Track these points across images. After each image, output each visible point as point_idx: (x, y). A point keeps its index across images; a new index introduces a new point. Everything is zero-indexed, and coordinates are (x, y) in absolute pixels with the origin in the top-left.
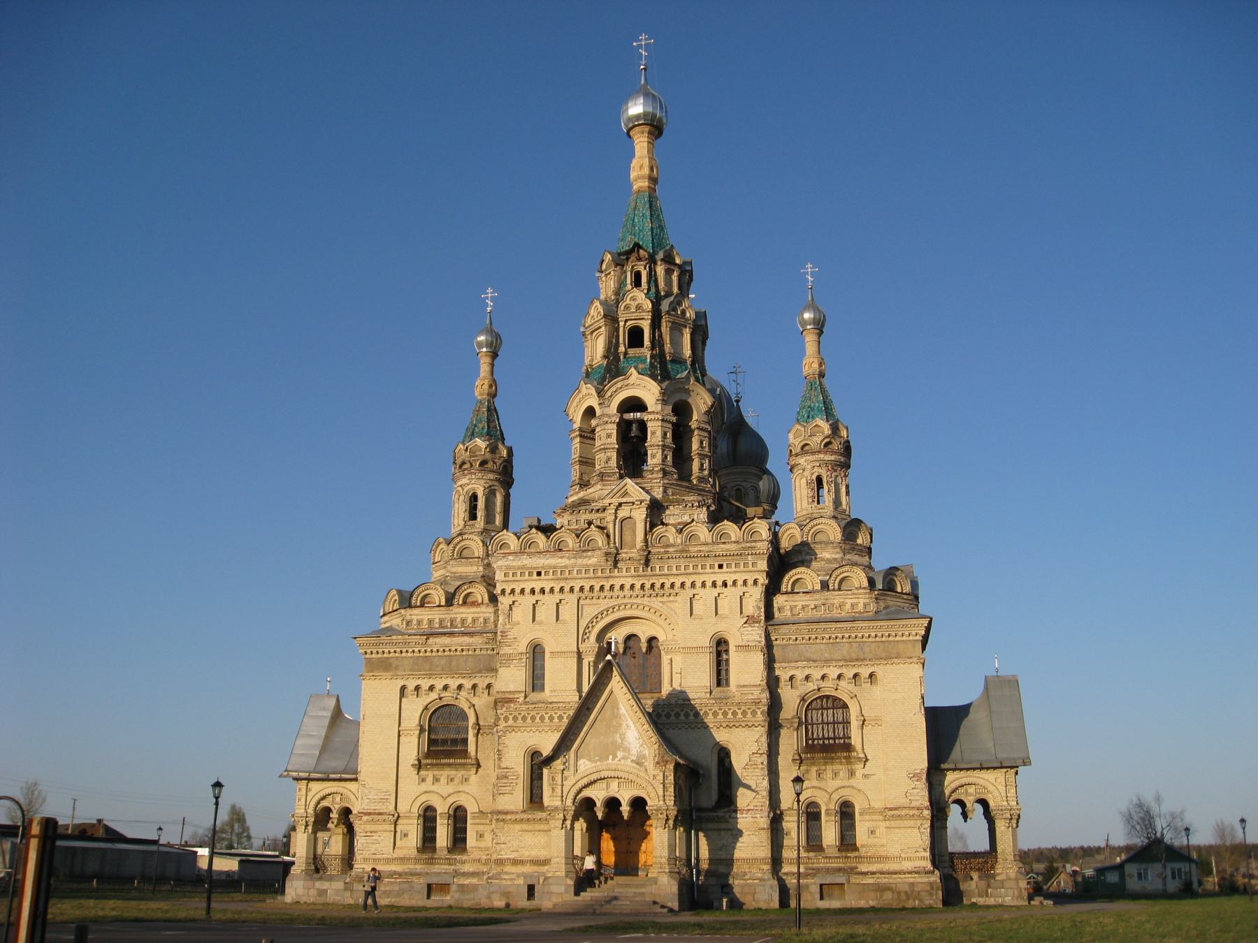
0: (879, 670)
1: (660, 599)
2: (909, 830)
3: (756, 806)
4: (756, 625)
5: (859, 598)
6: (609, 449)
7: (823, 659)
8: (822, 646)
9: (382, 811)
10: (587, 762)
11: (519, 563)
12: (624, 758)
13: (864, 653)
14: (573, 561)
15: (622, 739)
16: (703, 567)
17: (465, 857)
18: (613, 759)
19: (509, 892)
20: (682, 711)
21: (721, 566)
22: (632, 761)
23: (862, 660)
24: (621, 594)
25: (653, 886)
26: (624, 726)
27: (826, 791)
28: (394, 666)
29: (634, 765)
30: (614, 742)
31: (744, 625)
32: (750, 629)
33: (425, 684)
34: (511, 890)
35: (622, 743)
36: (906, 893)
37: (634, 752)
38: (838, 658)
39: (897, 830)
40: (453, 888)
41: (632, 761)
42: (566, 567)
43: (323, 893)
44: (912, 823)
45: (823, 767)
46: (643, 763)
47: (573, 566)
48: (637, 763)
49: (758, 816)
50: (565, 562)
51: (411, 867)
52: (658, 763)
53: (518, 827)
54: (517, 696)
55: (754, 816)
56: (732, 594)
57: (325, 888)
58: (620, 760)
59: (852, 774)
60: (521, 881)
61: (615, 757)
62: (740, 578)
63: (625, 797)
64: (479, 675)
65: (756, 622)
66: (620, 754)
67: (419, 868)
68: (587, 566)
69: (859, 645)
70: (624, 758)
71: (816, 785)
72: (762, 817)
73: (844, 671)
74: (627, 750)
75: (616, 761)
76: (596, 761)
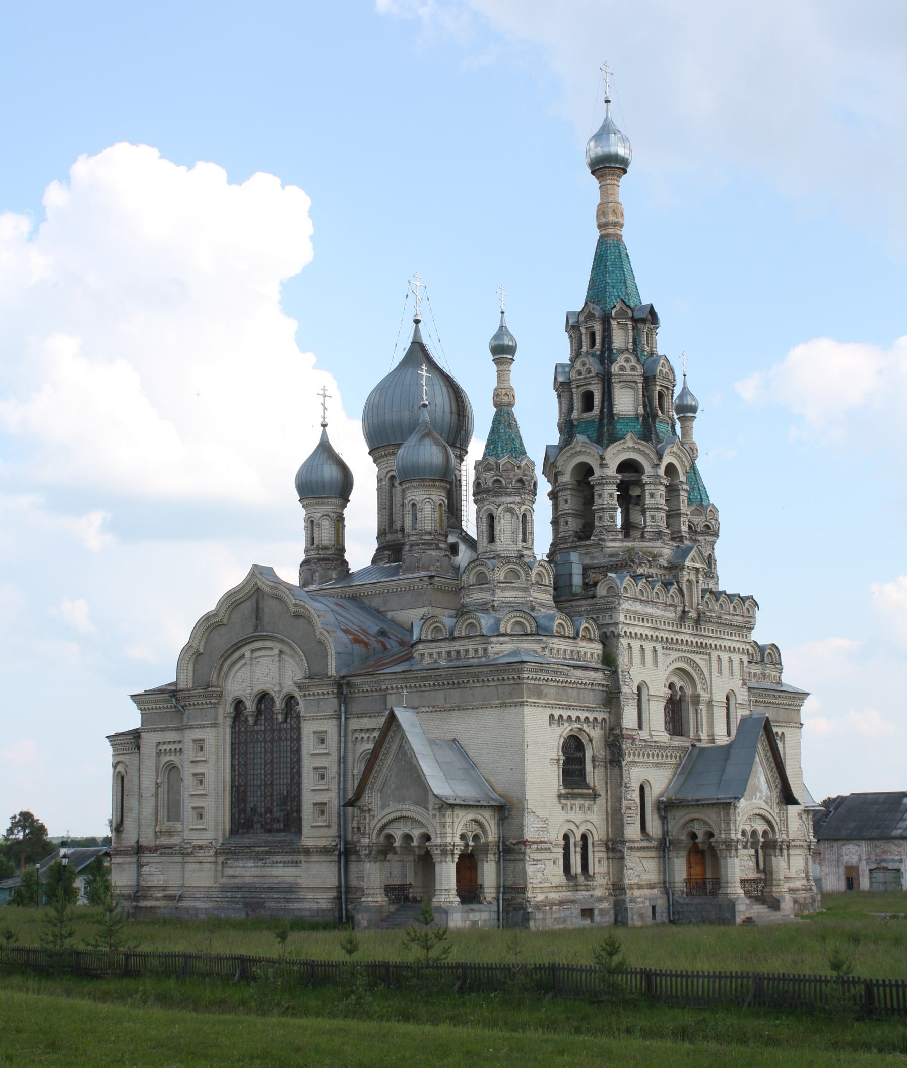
9: (543, 839)
11: (633, 609)
12: (760, 798)
15: (759, 782)
17: (595, 883)
19: (643, 914)
22: (764, 801)
28: (544, 693)
30: (755, 784)
33: (565, 713)
34: (643, 911)
37: (764, 794)
40: (596, 912)
43: (475, 923)
47: (662, 616)
51: (564, 894)
52: (778, 804)
53: (639, 854)
54: (634, 733)
57: (476, 919)
60: (647, 903)
61: (756, 797)
64: (598, 710)
66: (758, 795)
67: (568, 895)
70: (760, 798)
74: (761, 792)
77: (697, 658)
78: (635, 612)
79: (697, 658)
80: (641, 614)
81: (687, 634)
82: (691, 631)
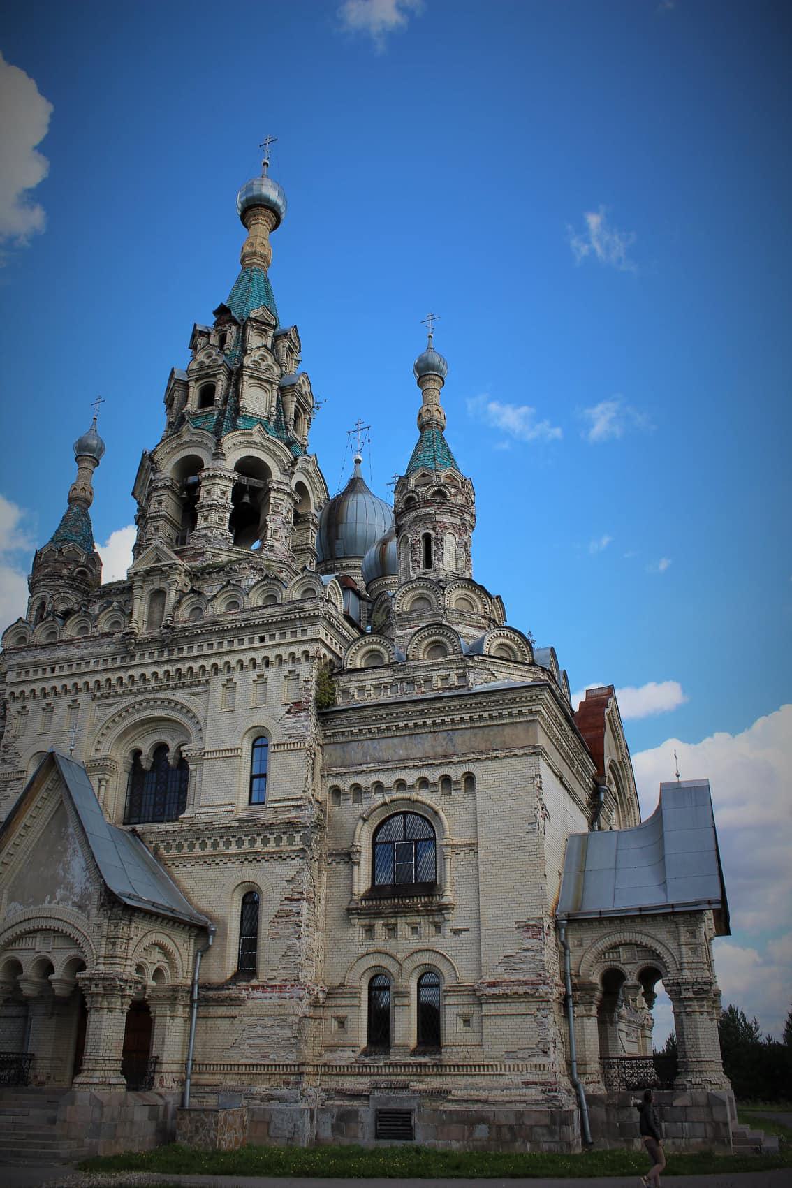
0: (476, 769)
1: (187, 690)
2: (519, 1020)
3: (286, 980)
4: (302, 714)
5: (448, 668)
6: (155, 517)
7: (397, 758)
8: (396, 740)
10: (19, 907)
12: (64, 899)
13: (454, 746)
14: (90, 650)
15: (66, 871)
16: (241, 641)
18: (50, 902)
20: (198, 839)
21: (262, 639)
22: (74, 903)
23: (452, 756)
24: (141, 686)
25: (69, 1108)
26: (70, 851)
27: (393, 958)
29: (74, 909)
31: (287, 715)
32: (294, 720)
35: (65, 877)
36: (511, 1128)
37: (77, 890)
38: (419, 755)
39: (499, 1020)
41: (74, 903)
42: (82, 659)
44: (522, 1008)
45: (393, 921)
46: (87, 906)
47: (90, 656)
48: (80, 907)
49: (287, 995)
50: (82, 652)
52: (102, 905)
55: (282, 995)
56: (275, 675)
58: (58, 903)
59: (438, 928)
61: (53, 897)
62: (285, 652)
63: (60, 960)
65: (304, 710)
66: (59, 893)
68: (106, 655)
69: (448, 734)
70: (64, 899)
71: (383, 949)
72: (292, 998)
73: (426, 773)
74: (69, 887)
75: (53, 905)
76: (28, 906)
77: (181, 696)
78: (36, 664)
79: (181, 696)
80: (47, 664)
81: (147, 666)
82: (156, 658)
